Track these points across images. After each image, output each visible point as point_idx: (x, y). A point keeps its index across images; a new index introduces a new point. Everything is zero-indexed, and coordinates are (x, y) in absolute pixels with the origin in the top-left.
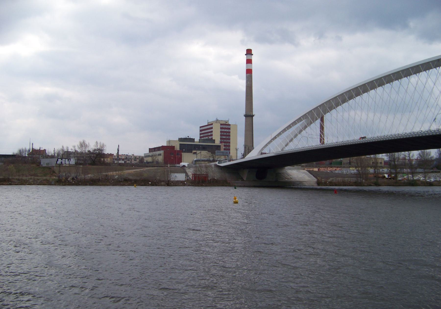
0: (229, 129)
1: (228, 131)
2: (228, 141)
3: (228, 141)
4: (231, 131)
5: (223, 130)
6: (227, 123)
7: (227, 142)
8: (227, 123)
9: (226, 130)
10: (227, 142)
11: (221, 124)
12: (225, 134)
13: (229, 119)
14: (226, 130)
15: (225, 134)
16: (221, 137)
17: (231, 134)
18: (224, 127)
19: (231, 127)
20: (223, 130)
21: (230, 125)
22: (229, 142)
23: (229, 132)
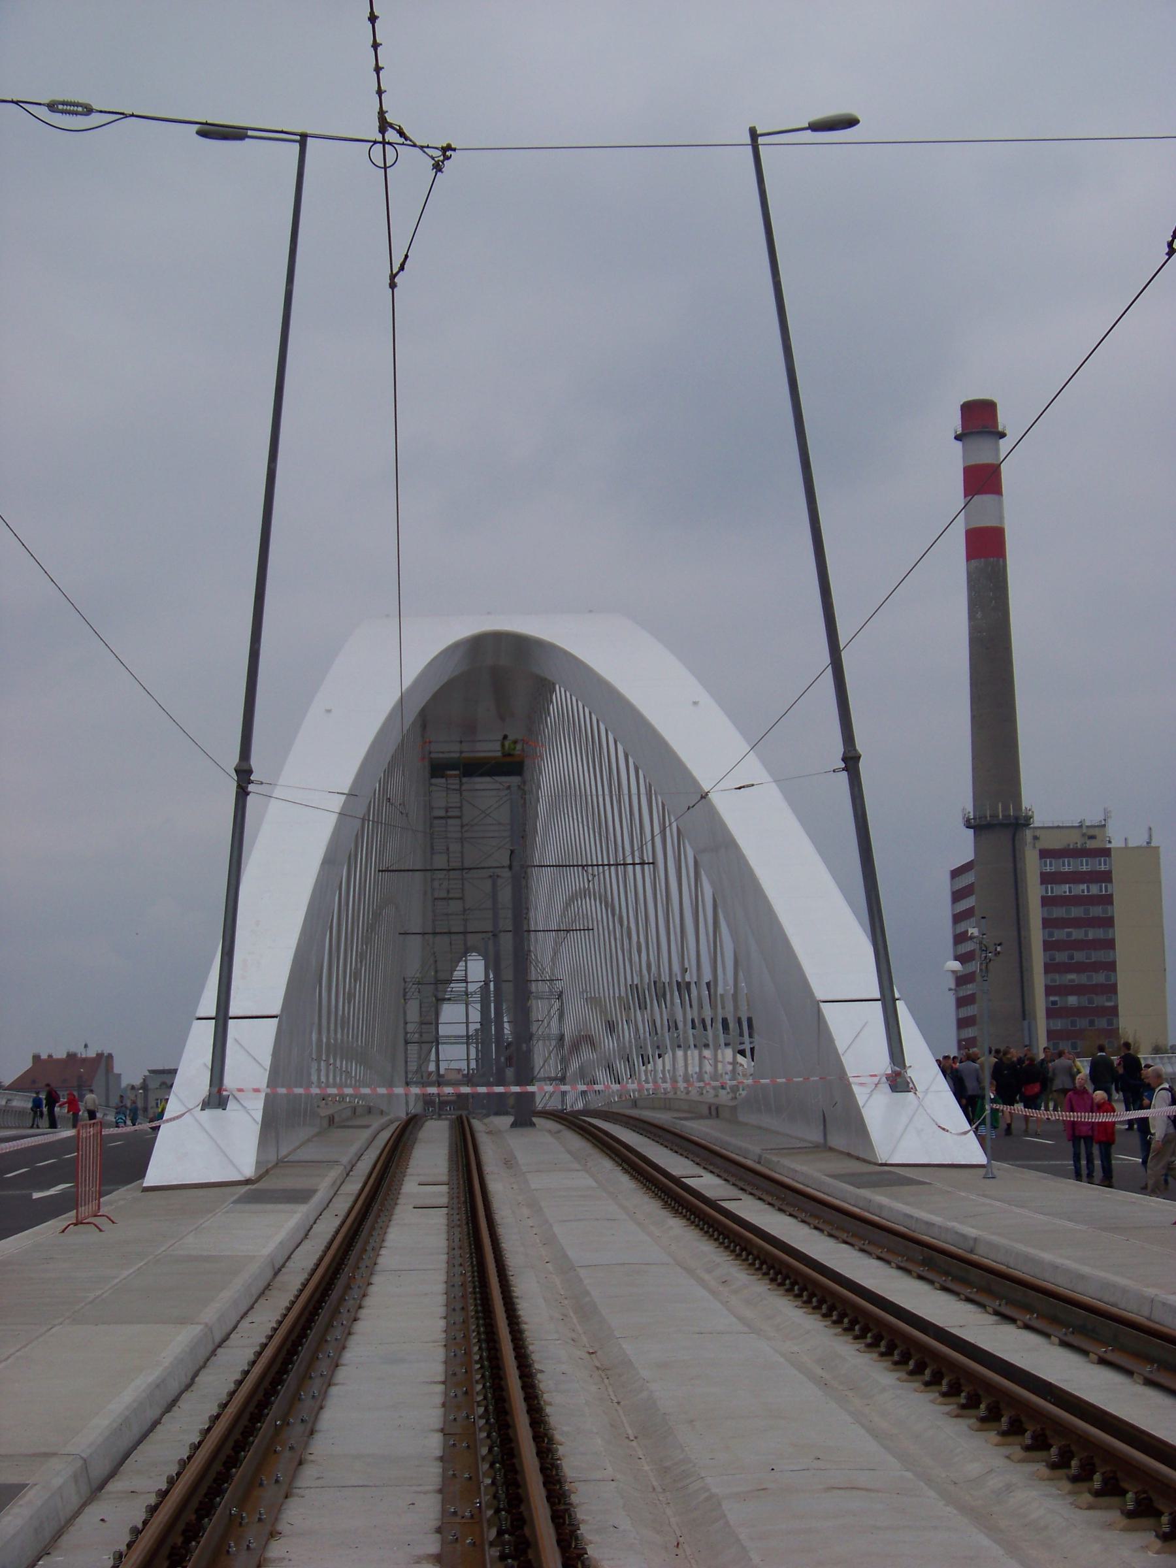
0: (1106, 877)
1: (1094, 889)
4: (1117, 889)
5: (1064, 889)
6: (1092, 837)
7: (1096, 967)
8: (1092, 837)
9: (1081, 889)
10: (1096, 967)
11: (1045, 854)
12: (1076, 912)
14: (1081, 889)
15: (1076, 912)
16: (1051, 935)
17: (1119, 910)
18: (1067, 866)
19: (1117, 866)
20: (1064, 889)
21: (1106, 853)
22: (1111, 966)
23: (1108, 900)
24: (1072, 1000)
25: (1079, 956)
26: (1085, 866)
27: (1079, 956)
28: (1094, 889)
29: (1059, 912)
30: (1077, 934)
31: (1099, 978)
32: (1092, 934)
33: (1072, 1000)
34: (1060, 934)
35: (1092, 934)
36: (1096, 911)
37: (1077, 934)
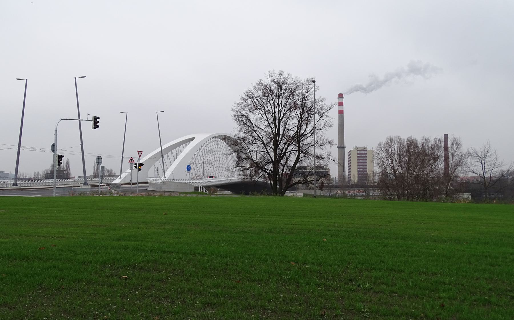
0: (366, 154)
1: (365, 155)
2: (365, 164)
3: (365, 164)
11: (358, 151)
12: (362, 158)
13: (367, 145)
15: (362, 158)
18: (361, 152)
19: (368, 152)
21: (366, 151)
24: (361, 170)
25: (362, 164)
26: (363, 152)
27: (362, 164)
28: (365, 155)
29: (360, 158)
30: (362, 161)
31: (365, 167)
32: (364, 161)
33: (361, 170)
34: (360, 161)
35: (364, 161)
36: (365, 158)
37: (362, 161)
